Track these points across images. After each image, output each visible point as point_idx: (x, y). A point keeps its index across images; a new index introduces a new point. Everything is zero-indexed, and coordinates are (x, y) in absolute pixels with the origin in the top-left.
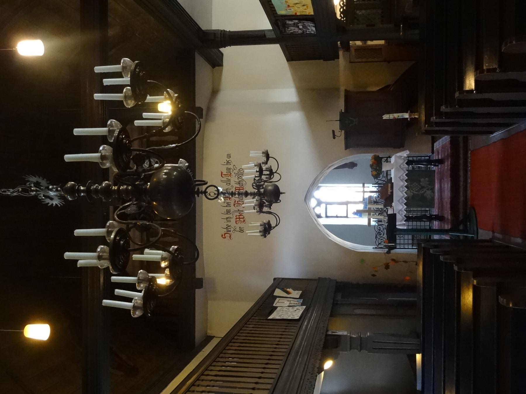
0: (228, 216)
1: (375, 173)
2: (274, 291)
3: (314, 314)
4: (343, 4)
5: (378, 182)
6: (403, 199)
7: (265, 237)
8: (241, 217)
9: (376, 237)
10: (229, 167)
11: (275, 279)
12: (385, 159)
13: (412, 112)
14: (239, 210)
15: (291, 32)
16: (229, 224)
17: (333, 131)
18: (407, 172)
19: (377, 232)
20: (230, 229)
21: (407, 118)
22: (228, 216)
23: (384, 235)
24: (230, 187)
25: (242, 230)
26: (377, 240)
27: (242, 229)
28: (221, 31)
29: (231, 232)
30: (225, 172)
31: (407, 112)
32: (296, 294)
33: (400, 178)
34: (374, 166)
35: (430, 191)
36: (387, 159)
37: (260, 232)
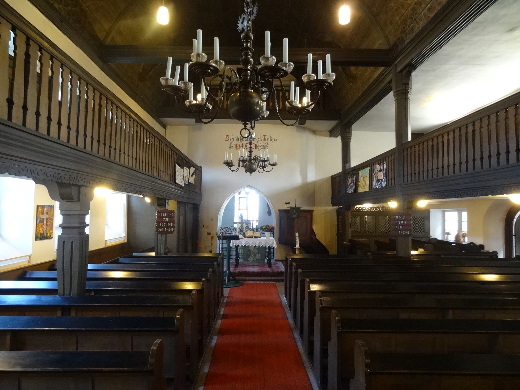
0: (240, 139)
1: (264, 228)
2: (193, 167)
3: (178, 192)
4: (364, 209)
6: (249, 244)
7: (224, 163)
8: (239, 147)
9: (227, 227)
10: (269, 140)
11: (201, 167)
12: (273, 233)
13: (299, 249)
14: (243, 146)
15: (349, 178)
16: (235, 140)
17: (289, 203)
18: (264, 246)
20: (231, 140)
21: (296, 247)
22: (240, 139)
24: (257, 140)
25: (231, 148)
27: (232, 148)
28: (351, 137)
29: (230, 141)
30: (266, 138)
31: (299, 247)
32: (192, 180)
33: (261, 242)
34: (268, 227)
35: (252, 260)
36: (272, 234)
37: (227, 160)
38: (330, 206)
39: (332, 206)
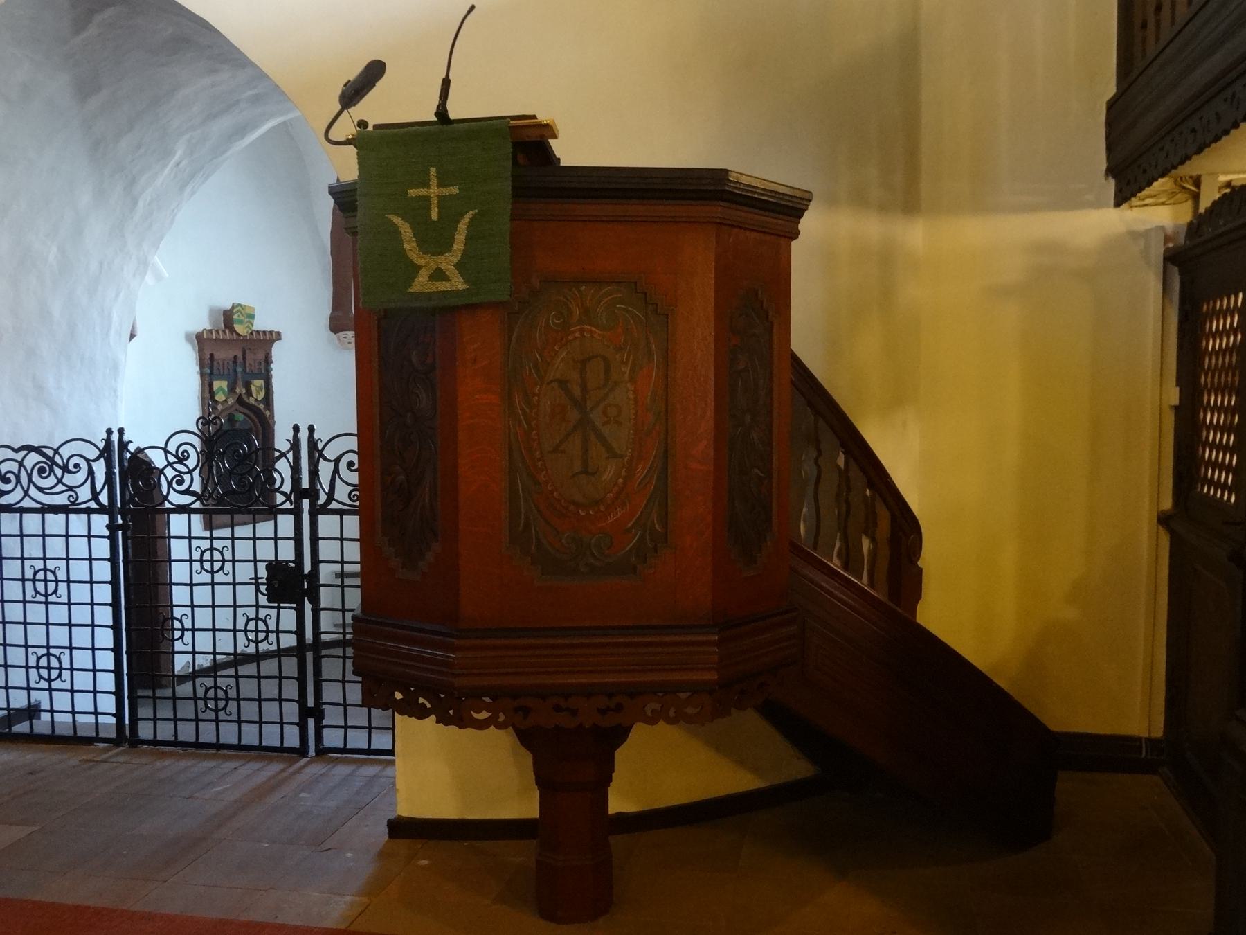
5: (326, 459)
9: (30, 449)
19: (56, 451)
23: (41, 490)
26: (11, 455)
38: (1097, 205)
39: (1121, 199)
